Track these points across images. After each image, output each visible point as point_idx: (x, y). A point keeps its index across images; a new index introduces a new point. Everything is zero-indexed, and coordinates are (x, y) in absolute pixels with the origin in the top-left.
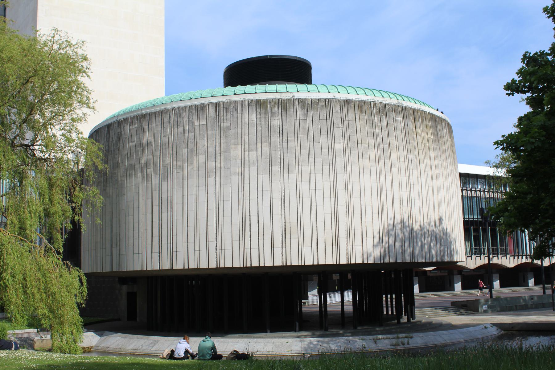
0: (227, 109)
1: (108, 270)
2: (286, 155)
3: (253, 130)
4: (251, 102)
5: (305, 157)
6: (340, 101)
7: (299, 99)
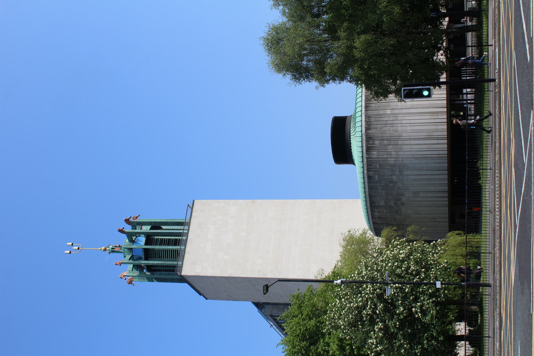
1: (447, 223)
4: (367, 154)
5: (394, 128)
6: (366, 110)
7: (365, 131)
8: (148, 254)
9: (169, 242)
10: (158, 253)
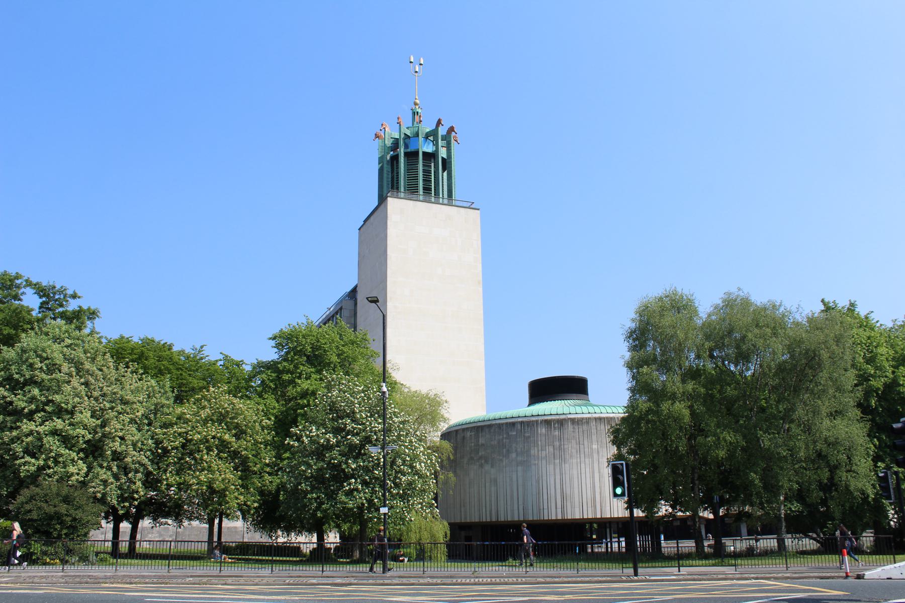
4: (542, 421)
6: (596, 419)
8: (412, 156)
9: (427, 181)
10: (413, 167)
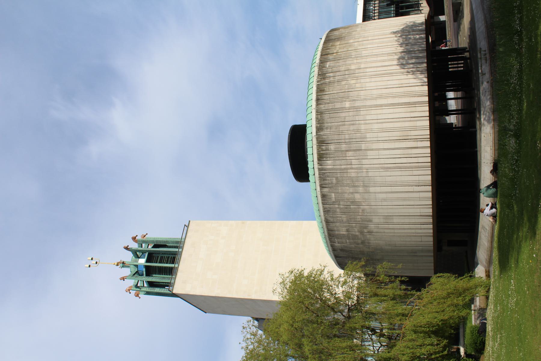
0: (324, 180)
1: (432, 259)
2: (354, 140)
3: (338, 162)
5: (355, 127)
6: (318, 104)
7: (317, 132)
8: (149, 271)
